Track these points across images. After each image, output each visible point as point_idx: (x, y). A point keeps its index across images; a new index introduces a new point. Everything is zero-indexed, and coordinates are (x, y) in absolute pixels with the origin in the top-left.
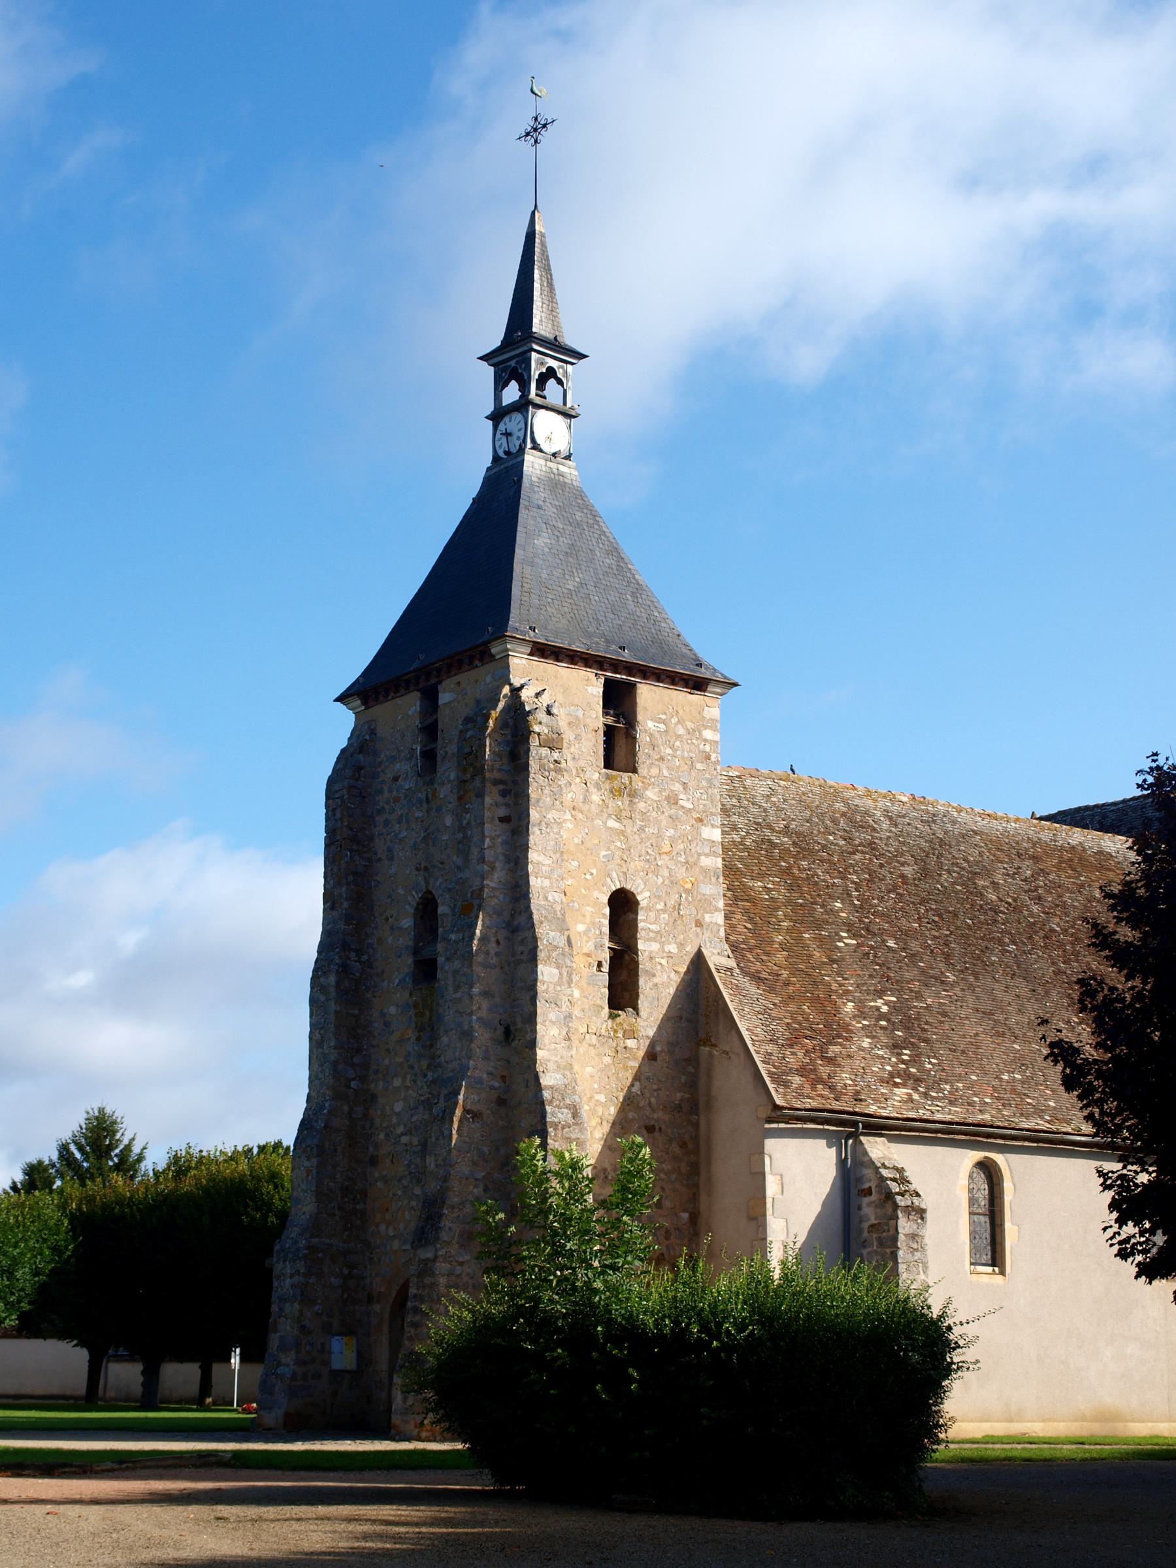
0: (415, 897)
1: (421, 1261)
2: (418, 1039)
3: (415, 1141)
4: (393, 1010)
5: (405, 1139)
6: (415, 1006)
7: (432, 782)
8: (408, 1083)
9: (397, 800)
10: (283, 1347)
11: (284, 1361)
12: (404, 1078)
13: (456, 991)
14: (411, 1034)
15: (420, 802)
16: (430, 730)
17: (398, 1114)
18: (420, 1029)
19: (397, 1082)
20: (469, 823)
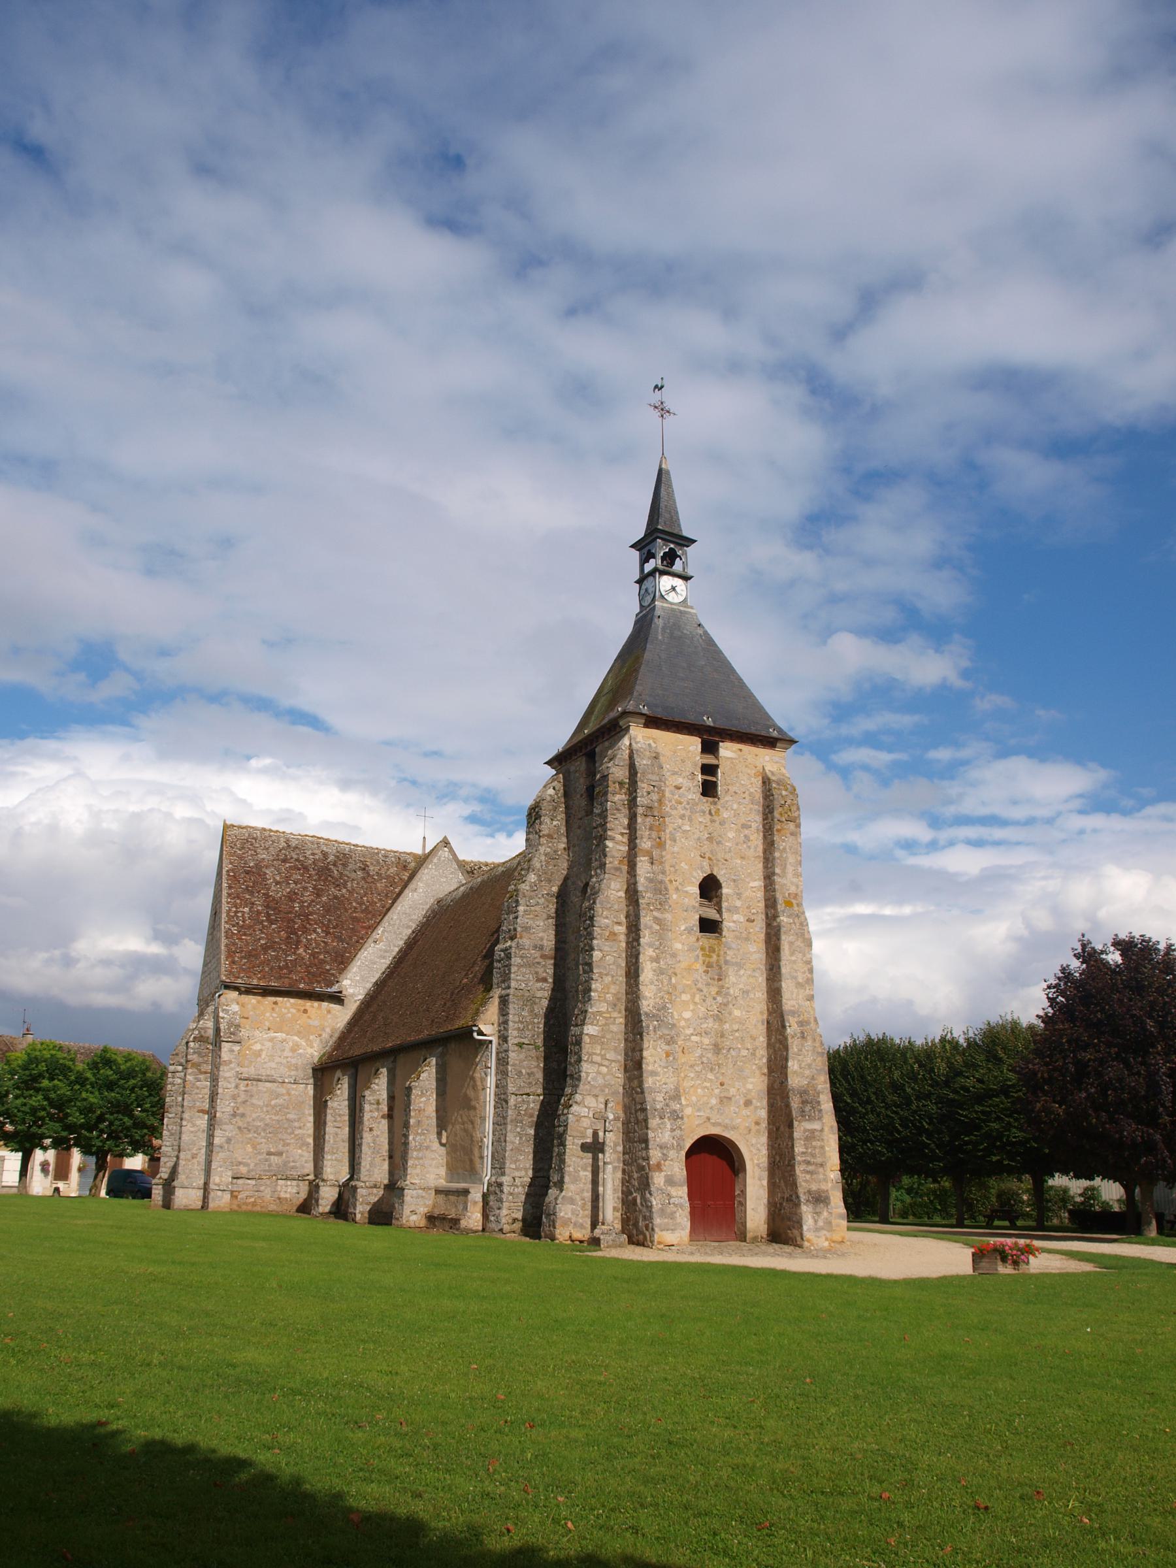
0: (700, 876)
1: (805, 1130)
2: (706, 972)
3: (706, 1041)
4: (678, 946)
5: (693, 1038)
6: (702, 949)
7: (715, 803)
8: (697, 999)
9: (681, 803)
10: (670, 1181)
11: (674, 1193)
12: (693, 996)
13: (792, 954)
14: (700, 967)
15: (704, 812)
16: (709, 770)
17: (687, 1020)
18: (709, 965)
19: (685, 997)
20: (785, 849)
